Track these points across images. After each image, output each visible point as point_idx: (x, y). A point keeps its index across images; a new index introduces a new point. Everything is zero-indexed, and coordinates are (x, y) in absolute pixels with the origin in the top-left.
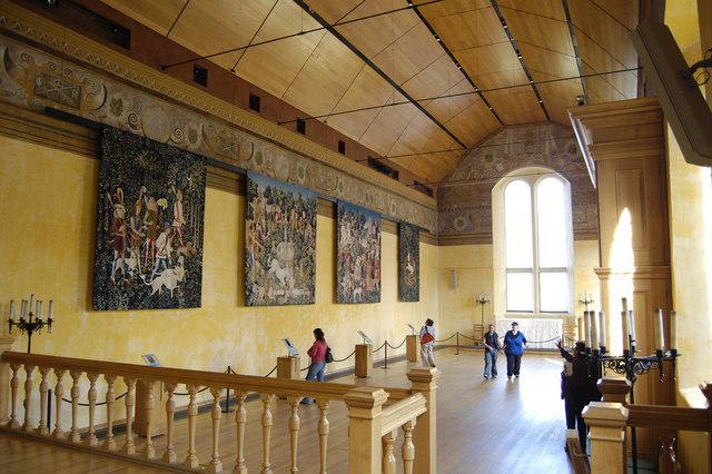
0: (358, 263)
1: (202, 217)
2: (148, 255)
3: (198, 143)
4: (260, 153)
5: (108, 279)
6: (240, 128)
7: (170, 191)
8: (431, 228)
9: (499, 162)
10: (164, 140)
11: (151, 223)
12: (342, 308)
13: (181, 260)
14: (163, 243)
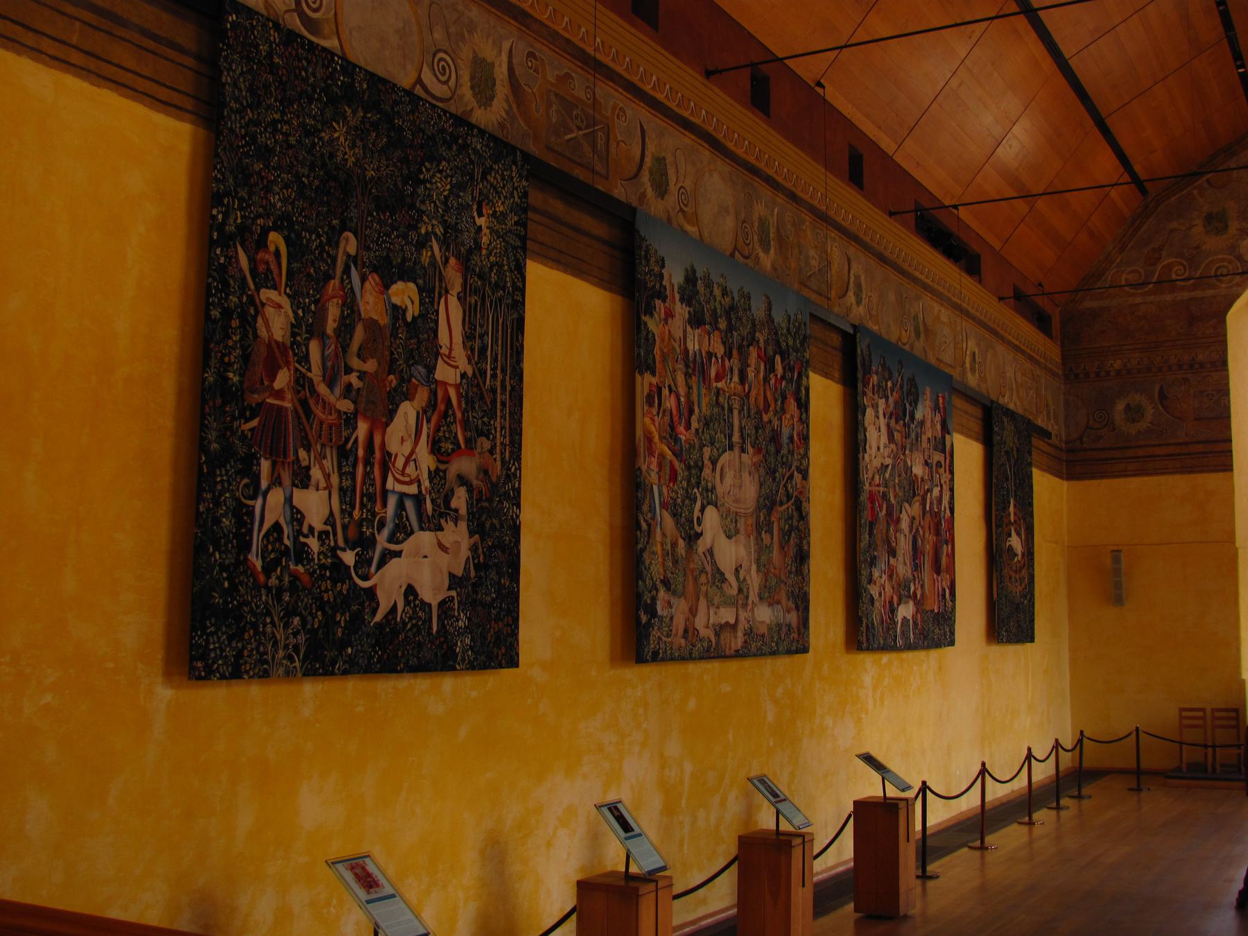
0: (904, 525)
1: (518, 353)
2: (363, 472)
4: (660, 161)
5: (242, 562)
6: (611, 75)
7: (425, 257)
8: (1050, 426)
10: (406, 81)
11: (370, 366)
12: (868, 661)
13: (460, 500)
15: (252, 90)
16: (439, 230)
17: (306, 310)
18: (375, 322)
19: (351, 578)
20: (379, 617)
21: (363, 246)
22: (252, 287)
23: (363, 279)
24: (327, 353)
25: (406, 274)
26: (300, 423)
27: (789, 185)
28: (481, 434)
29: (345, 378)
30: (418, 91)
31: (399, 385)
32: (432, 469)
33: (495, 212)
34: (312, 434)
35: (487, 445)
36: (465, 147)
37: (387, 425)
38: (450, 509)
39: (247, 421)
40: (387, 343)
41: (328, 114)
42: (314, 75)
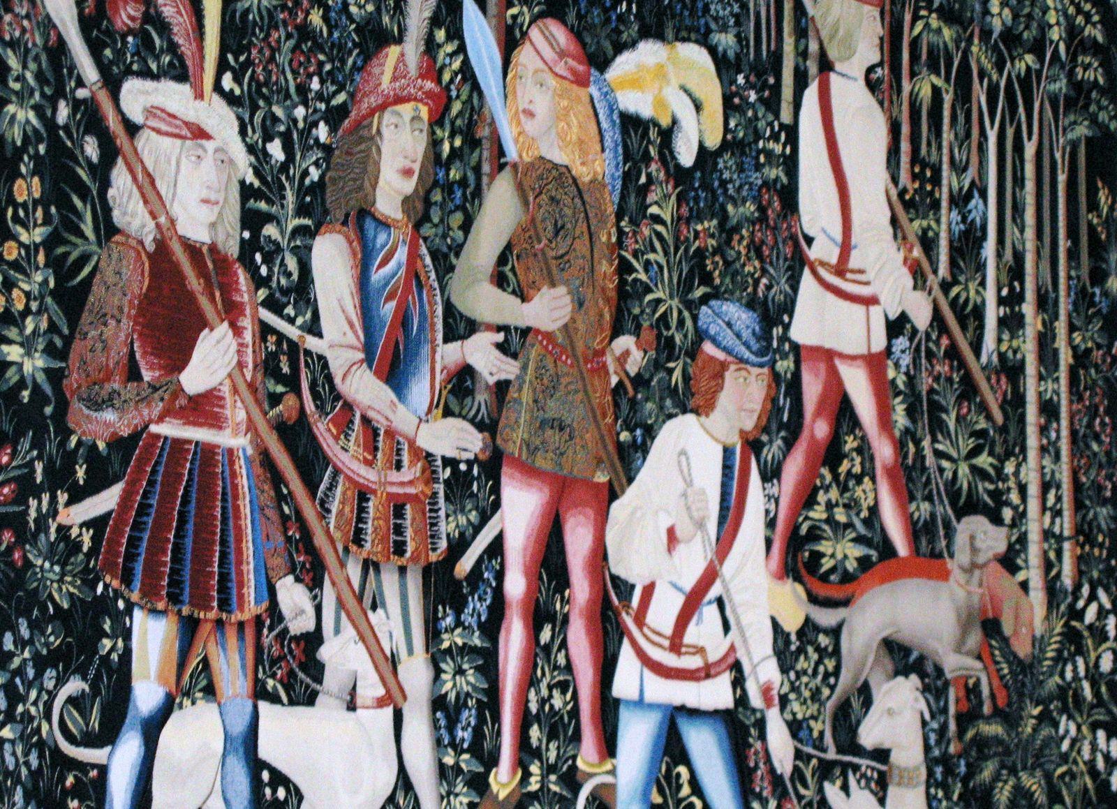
11: (548, 309)
18: (561, 174)
22: (90, 72)
24: (377, 276)
26: (280, 498)
28: (967, 506)
29: (450, 354)
31: (657, 365)
32: (791, 625)
34: (327, 534)
35: (993, 539)
37: (613, 494)
38: (858, 750)
39: (77, 496)
40: (607, 235)
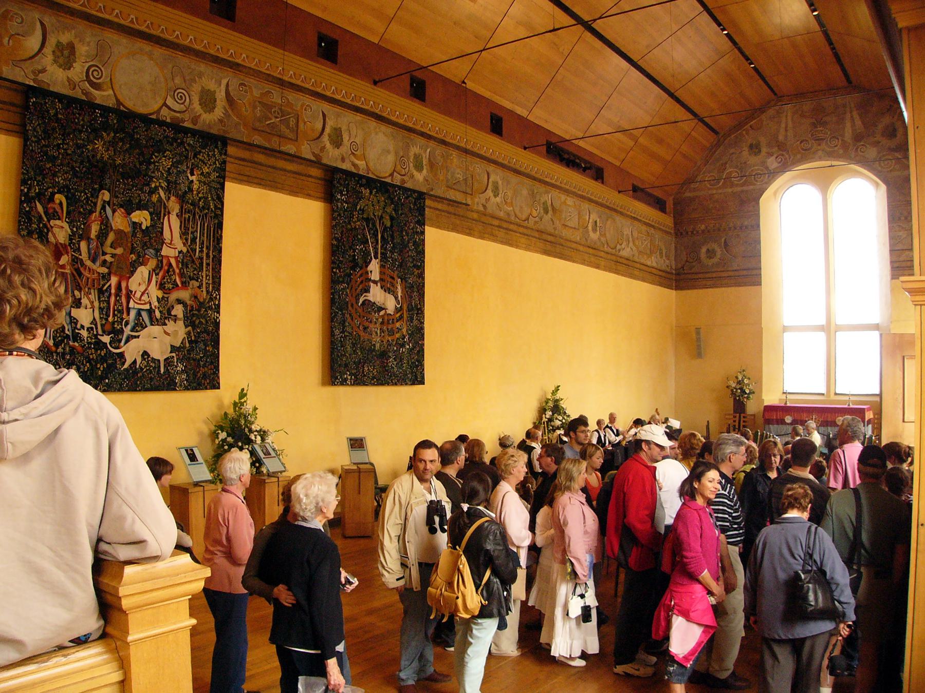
1: (219, 240)
3: (219, 112)
7: (155, 198)
9: (770, 154)
11: (119, 251)
14: (143, 285)
15: (44, 132)
16: (164, 184)
17: (78, 228)
19: (107, 348)
20: (126, 366)
21: (114, 195)
23: (114, 211)
25: (140, 207)
27: (440, 136)
28: (192, 279)
29: (103, 258)
30: (165, 112)
32: (160, 296)
33: (203, 173)
35: (196, 284)
36: (182, 143)
37: (130, 277)
41: (91, 137)
42: (83, 120)
